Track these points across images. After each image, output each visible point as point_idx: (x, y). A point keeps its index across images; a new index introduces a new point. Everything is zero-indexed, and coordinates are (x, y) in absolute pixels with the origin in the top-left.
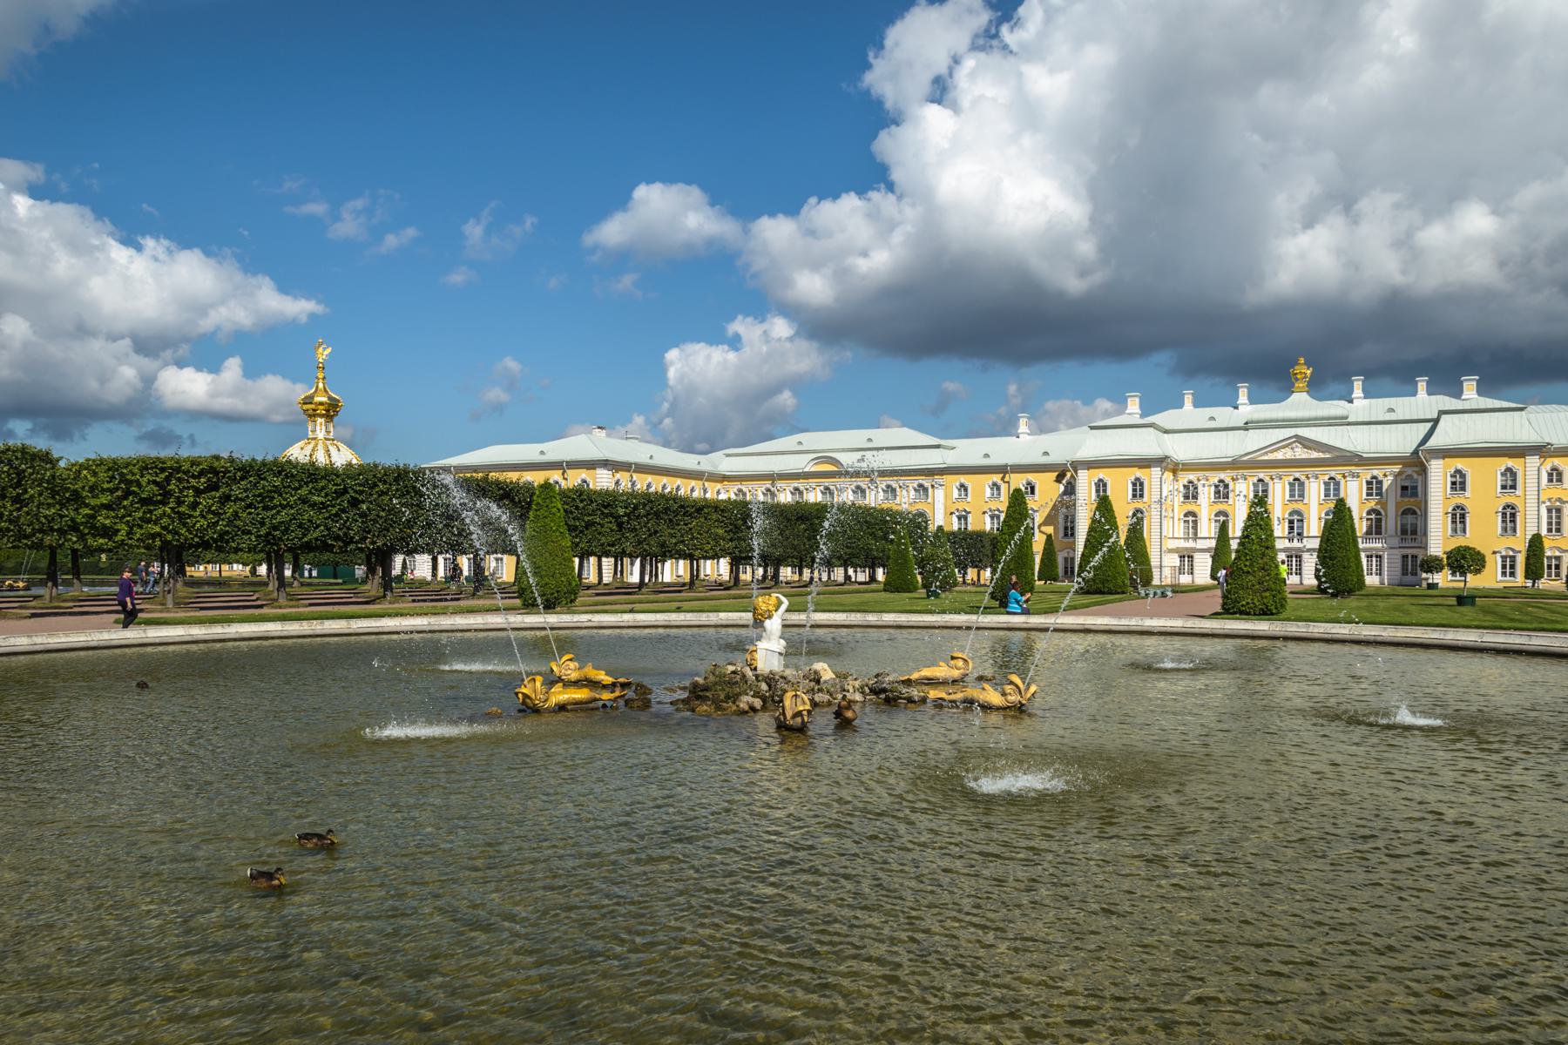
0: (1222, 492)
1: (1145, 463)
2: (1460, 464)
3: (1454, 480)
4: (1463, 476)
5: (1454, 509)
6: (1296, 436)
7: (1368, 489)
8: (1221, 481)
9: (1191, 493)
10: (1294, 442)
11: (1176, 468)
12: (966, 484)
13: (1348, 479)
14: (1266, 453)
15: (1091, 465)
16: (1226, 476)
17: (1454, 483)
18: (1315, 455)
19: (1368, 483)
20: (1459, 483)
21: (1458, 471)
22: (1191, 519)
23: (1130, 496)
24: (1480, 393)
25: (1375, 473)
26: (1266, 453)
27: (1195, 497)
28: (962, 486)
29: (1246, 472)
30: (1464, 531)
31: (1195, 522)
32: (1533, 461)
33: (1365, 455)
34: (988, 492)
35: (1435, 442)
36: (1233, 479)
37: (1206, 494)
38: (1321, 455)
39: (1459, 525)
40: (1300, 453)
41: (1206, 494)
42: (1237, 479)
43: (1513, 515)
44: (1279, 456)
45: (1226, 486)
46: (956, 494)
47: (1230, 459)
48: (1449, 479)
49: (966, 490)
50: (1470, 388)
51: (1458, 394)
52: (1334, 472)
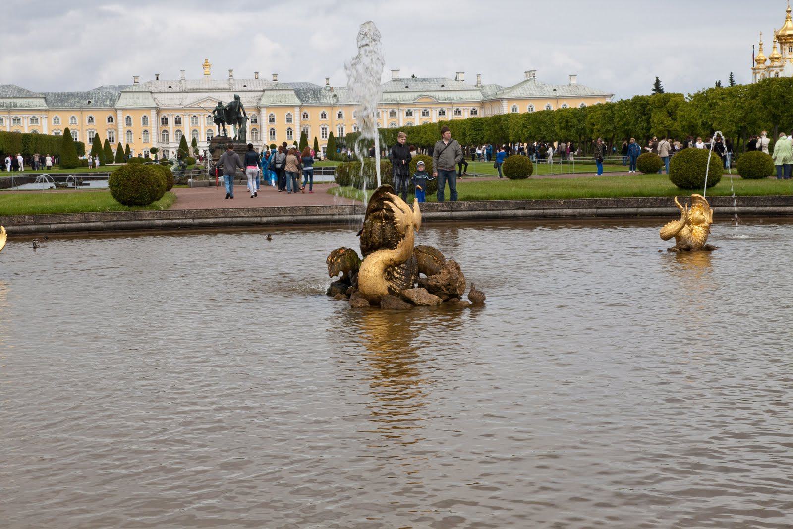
0: (178, 121)
8: (178, 116)
9: (165, 121)
11: (158, 111)
12: (58, 117)
16: (179, 114)
20: (272, 121)
22: (165, 133)
27: (167, 123)
28: (56, 117)
29: (189, 112)
30: (274, 138)
35: (263, 102)
37: (171, 121)
41: (171, 121)
43: (291, 132)
45: (180, 119)
49: (58, 120)
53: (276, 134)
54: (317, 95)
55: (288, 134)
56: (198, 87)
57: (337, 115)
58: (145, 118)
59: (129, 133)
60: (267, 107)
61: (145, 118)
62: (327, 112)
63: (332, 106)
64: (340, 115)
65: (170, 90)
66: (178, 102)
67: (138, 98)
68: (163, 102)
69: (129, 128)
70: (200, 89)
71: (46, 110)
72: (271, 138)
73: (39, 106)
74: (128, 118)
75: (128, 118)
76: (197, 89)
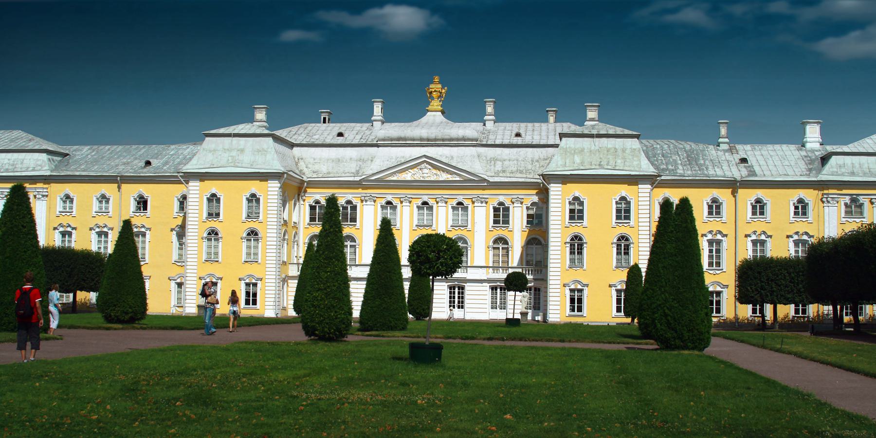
1: (264, 177)
2: (577, 190)
3: (572, 207)
4: (581, 204)
5: (572, 239)
6: (425, 156)
7: (495, 216)
10: (425, 161)
13: (476, 204)
14: (394, 173)
15: (203, 177)
17: (572, 211)
18: (444, 177)
19: (496, 210)
20: (576, 215)
21: (576, 199)
23: (244, 215)
24: (601, 119)
25: (502, 199)
26: (394, 173)
31: (354, 246)
32: (645, 188)
33: (491, 180)
34: (95, 206)
36: (362, 201)
38: (450, 177)
39: (576, 256)
40: (428, 174)
42: (366, 201)
44: (408, 176)
46: (59, 206)
47: (357, 179)
48: (568, 207)
50: (592, 114)
51: (581, 120)
52: (461, 195)
53: (585, 251)
54: (696, 160)
55: (619, 253)
56: (403, 135)
57: (750, 208)
58: (253, 199)
59: (213, 237)
60: (565, 179)
61: (253, 199)
62: (723, 195)
63: (734, 185)
64: (759, 207)
65: (340, 140)
66: (353, 167)
67: (242, 151)
68: (316, 167)
69: (213, 224)
70: (405, 139)
71: (47, 180)
72: (572, 261)
73: (33, 170)
74: (213, 199)
75: (213, 199)
76: (399, 139)
